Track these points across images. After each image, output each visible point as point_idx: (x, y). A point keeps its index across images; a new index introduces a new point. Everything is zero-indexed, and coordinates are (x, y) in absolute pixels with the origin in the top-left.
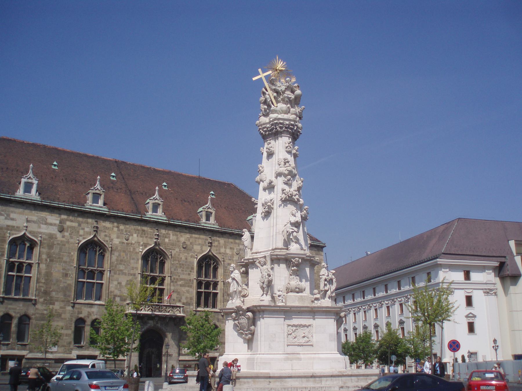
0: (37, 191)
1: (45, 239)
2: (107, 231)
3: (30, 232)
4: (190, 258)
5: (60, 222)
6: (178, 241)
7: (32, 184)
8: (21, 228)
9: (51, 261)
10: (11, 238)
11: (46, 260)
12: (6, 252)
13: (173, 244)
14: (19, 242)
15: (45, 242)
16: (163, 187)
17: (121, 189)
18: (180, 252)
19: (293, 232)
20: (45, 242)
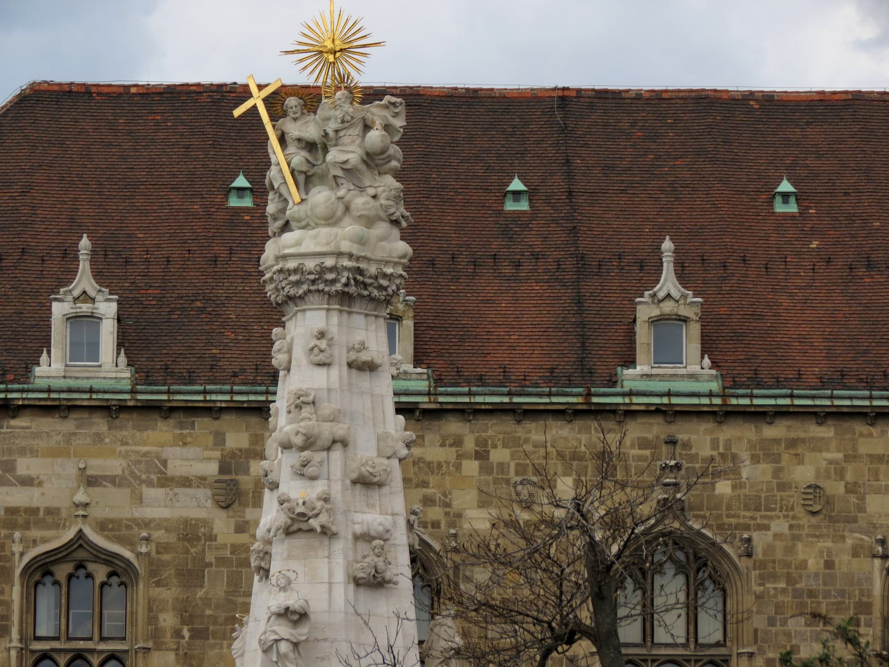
0: (120, 345)
1: (163, 548)
2: (432, 480)
3: (102, 526)
4: (846, 558)
5: (224, 468)
6: (782, 486)
7: (94, 319)
8: (64, 514)
9: (197, 634)
10: (26, 559)
11: (178, 634)
12: (16, 618)
13: (754, 504)
14: (62, 571)
15: (166, 557)
16: (778, 199)
17: (536, 257)
18: (796, 538)
19: (276, 641)
20: (166, 557)
